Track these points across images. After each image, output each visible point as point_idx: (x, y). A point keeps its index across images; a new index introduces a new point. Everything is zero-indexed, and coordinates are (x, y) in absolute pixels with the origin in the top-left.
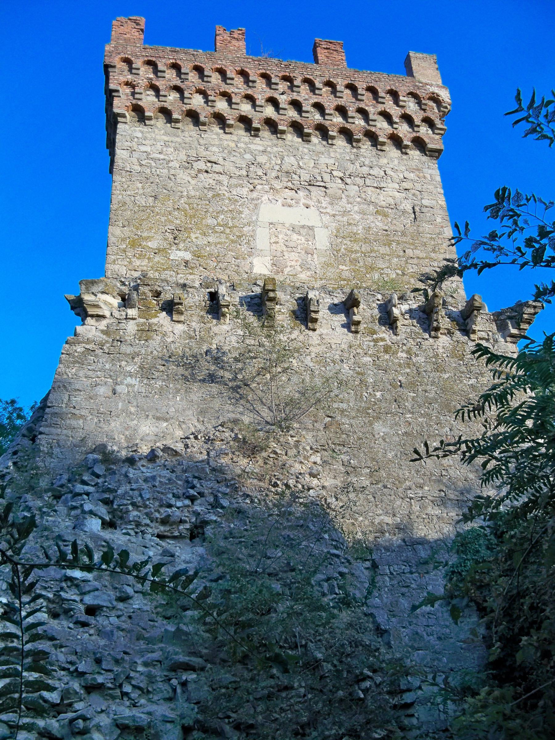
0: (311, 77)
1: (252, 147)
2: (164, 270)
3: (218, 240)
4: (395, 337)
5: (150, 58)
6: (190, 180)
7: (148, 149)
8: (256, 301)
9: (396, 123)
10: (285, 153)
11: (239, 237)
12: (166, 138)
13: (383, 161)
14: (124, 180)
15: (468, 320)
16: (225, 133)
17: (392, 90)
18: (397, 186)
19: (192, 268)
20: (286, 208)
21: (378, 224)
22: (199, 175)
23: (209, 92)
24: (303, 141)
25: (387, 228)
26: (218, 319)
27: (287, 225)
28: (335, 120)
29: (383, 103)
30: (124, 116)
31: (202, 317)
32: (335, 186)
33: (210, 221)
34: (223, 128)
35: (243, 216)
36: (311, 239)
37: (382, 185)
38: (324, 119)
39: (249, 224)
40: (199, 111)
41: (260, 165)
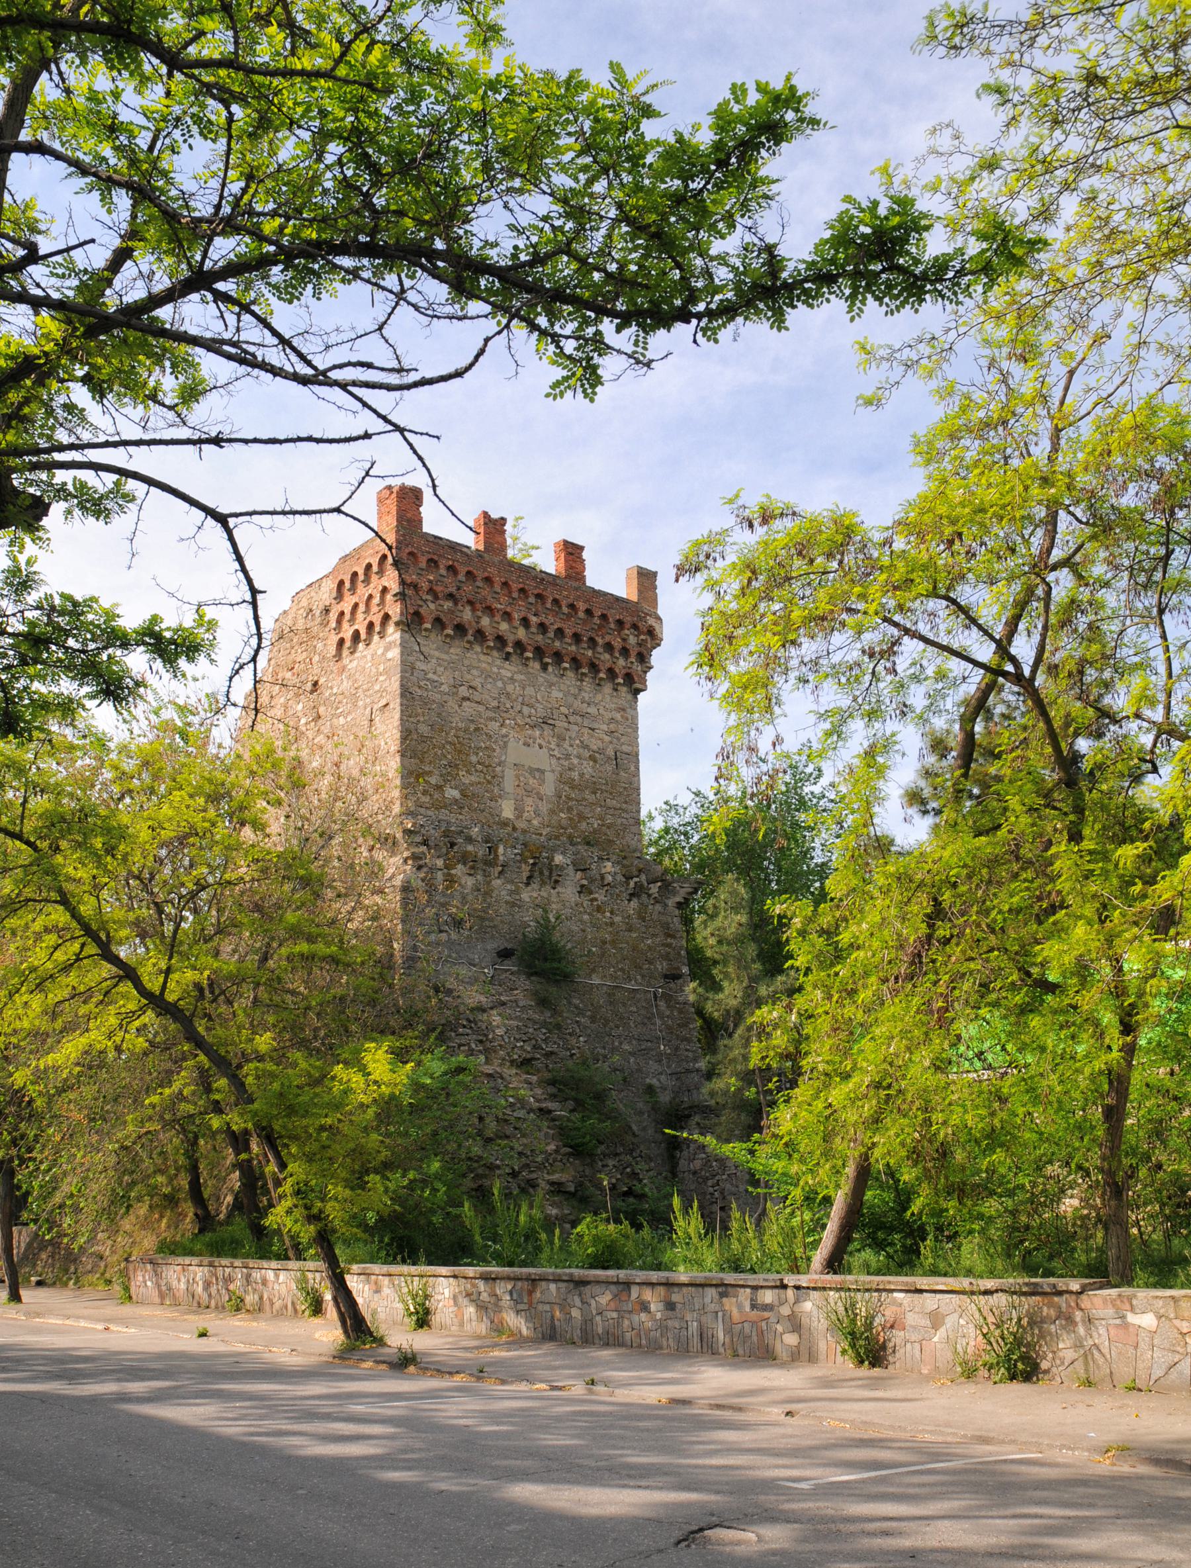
12: (437, 654)
13: (599, 697)
32: (561, 724)
33: (474, 759)
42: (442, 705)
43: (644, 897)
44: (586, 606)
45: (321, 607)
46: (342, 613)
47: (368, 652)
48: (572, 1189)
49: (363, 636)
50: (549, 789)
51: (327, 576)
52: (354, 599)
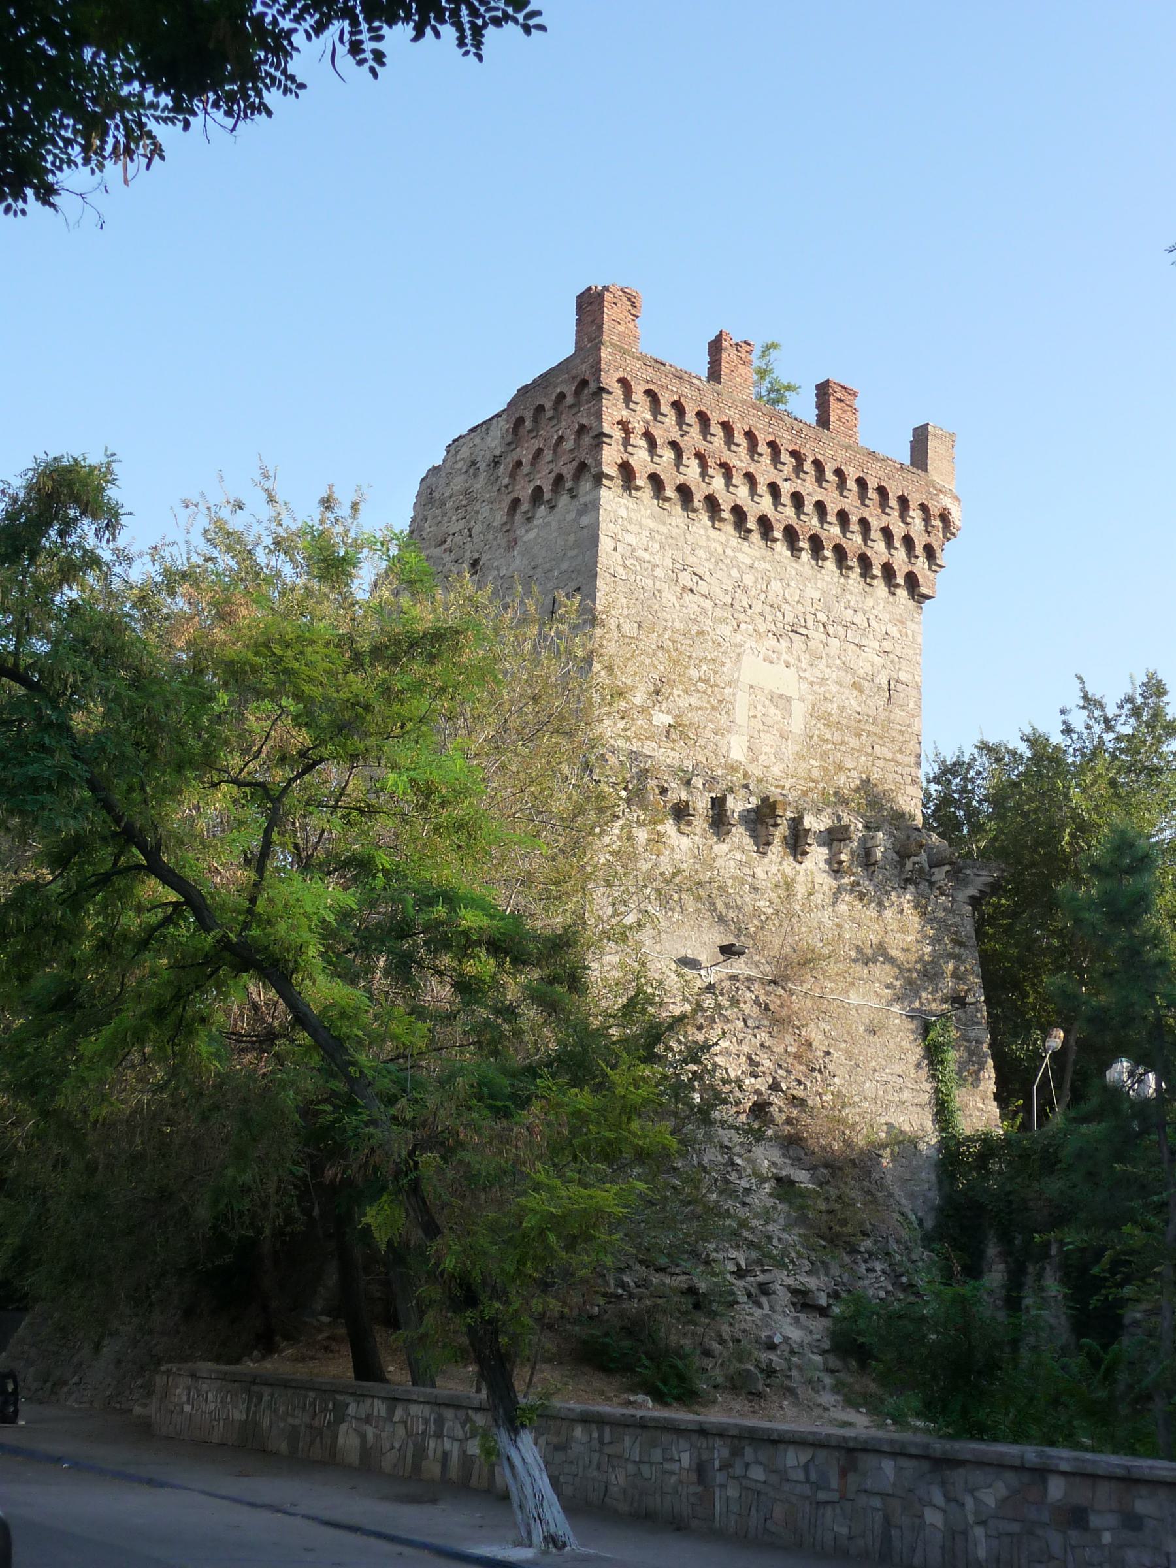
2: (647, 739)
3: (699, 704)
5: (653, 387)
7: (630, 538)
9: (896, 549)
11: (721, 702)
12: (652, 524)
13: (870, 602)
16: (713, 526)
18: (876, 645)
20: (767, 664)
21: (852, 702)
22: (684, 595)
23: (710, 462)
25: (859, 710)
26: (718, 835)
27: (766, 692)
28: (832, 530)
30: (610, 478)
32: (817, 635)
33: (693, 673)
34: (712, 519)
35: (725, 670)
36: (787, 716)
38: (822, 527)
39: (729, 684)
40: (693, 489)
42: (657, 594)
43: (924, 886)
45: (489, 456)
46: (519, 464)
47: (553, 519)
48: (823, 1301)
49: (547, 496)
50: (797, 723)
51: (498, 416)
52: (536, 444)
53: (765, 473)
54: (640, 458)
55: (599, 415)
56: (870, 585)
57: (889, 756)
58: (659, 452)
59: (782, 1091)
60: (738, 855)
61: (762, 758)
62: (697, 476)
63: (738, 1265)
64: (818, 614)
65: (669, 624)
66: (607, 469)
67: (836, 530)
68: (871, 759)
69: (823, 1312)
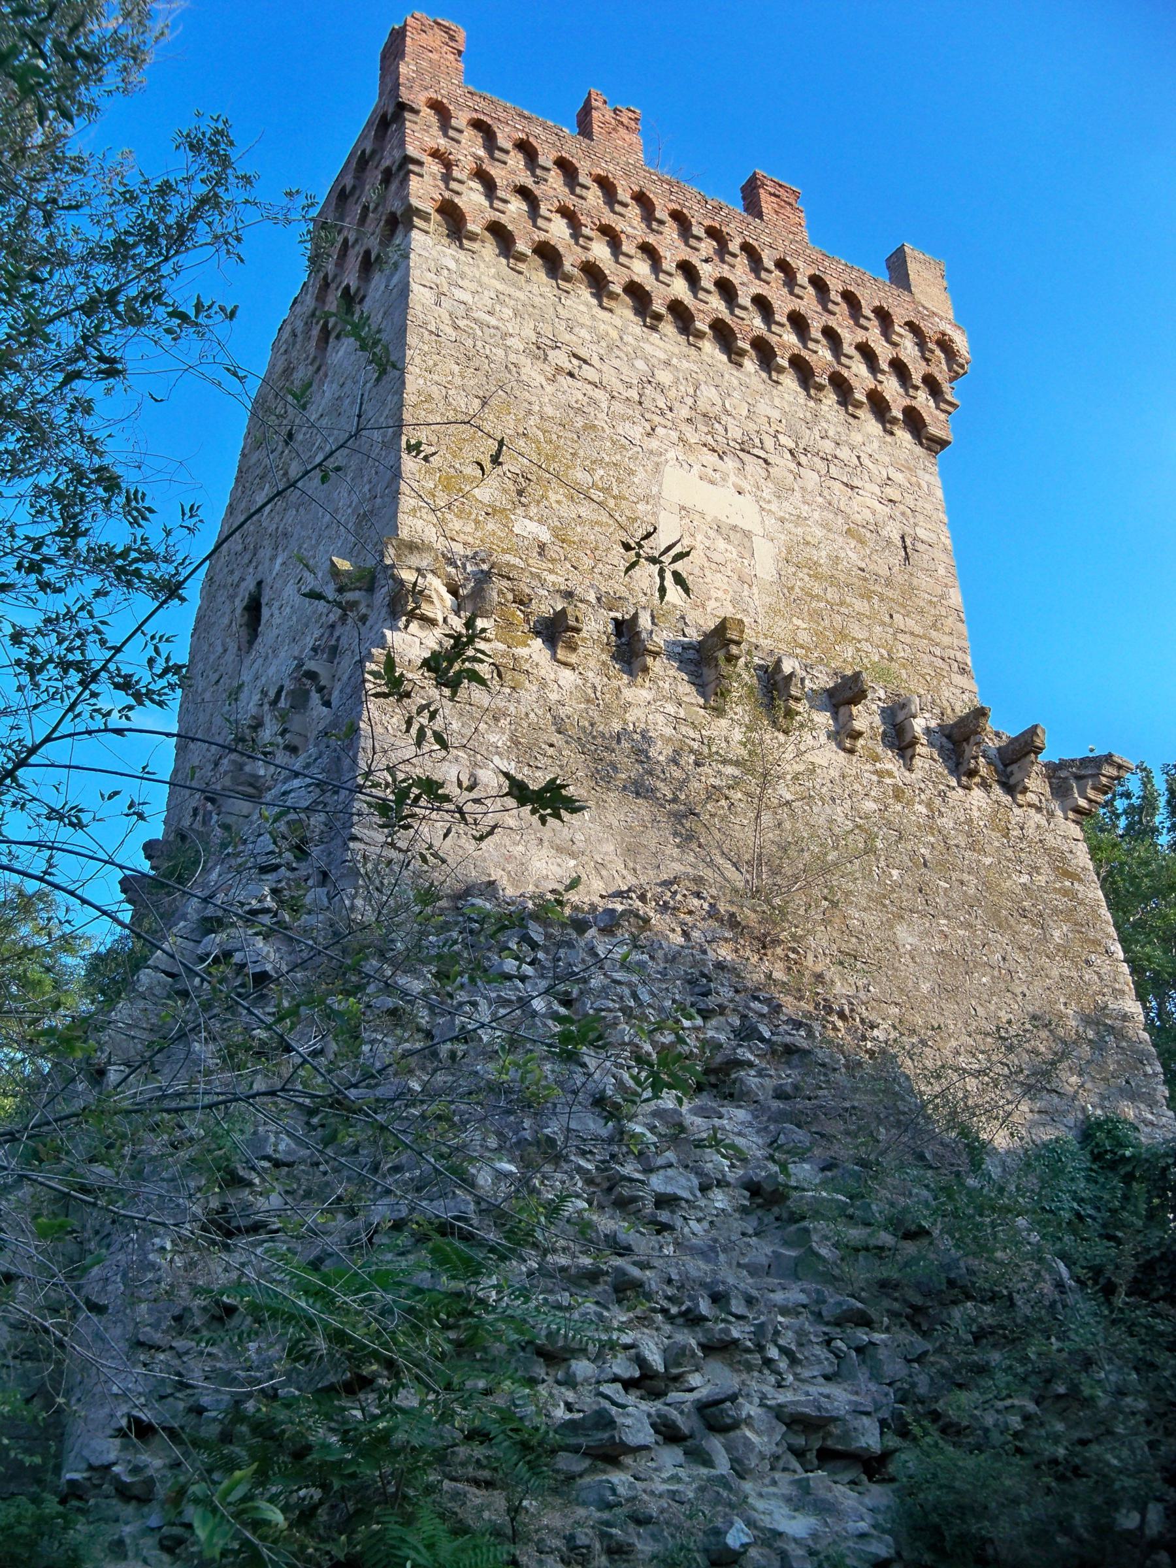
0: (755, 243)
1: (646, 346)
3: (595, 517)
4: (907, 773)
5: (482, 117)
6: (544, 383)
7: (466, 297)
8: (691, 654)
10: (702, 377)
12: (500, 287)
13: (857, 438)
14: (426, 348)
15: (1014, 767)
16: (601, 305)
17: (882, 308)
18: (877, 490)
19: (553, 561)
20: (704, 484)
23: (583, 219)
24: (730, 361)
25: (863, 565)
26: (631, 673)
27: (709, 519)
28: (785, 337)
29: (866, 329)
30: (426, 217)
31: (604, 663)
34: (598, 296)
37: (856, 482)
38: (769, 330)
39: (646, 499)
40: (561, 250)
41: (661, 388)
44: (811, 271)
48: (870, 1439)
50: (766, 561)
53: (671, 247)
54: (472, 198)
55: (402, 143)
56: (855, 417)
57: (918, 630)
58: (500, 193)
59: (762, 1039)
60: (671, 708)
61: (711, 604)
62: (567, 237)
63: (641, 1361)
64: (780, 436)
65: (536, 408)
66: (414, 202)
67: (790, 338)
68: (891, 631)
69: (872, 1466)
